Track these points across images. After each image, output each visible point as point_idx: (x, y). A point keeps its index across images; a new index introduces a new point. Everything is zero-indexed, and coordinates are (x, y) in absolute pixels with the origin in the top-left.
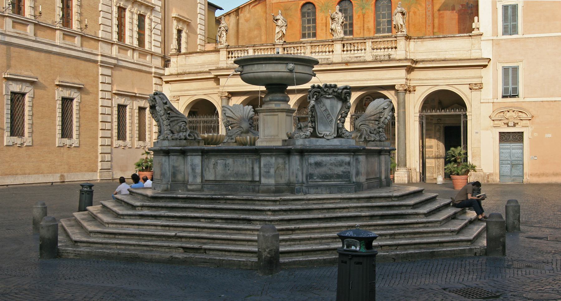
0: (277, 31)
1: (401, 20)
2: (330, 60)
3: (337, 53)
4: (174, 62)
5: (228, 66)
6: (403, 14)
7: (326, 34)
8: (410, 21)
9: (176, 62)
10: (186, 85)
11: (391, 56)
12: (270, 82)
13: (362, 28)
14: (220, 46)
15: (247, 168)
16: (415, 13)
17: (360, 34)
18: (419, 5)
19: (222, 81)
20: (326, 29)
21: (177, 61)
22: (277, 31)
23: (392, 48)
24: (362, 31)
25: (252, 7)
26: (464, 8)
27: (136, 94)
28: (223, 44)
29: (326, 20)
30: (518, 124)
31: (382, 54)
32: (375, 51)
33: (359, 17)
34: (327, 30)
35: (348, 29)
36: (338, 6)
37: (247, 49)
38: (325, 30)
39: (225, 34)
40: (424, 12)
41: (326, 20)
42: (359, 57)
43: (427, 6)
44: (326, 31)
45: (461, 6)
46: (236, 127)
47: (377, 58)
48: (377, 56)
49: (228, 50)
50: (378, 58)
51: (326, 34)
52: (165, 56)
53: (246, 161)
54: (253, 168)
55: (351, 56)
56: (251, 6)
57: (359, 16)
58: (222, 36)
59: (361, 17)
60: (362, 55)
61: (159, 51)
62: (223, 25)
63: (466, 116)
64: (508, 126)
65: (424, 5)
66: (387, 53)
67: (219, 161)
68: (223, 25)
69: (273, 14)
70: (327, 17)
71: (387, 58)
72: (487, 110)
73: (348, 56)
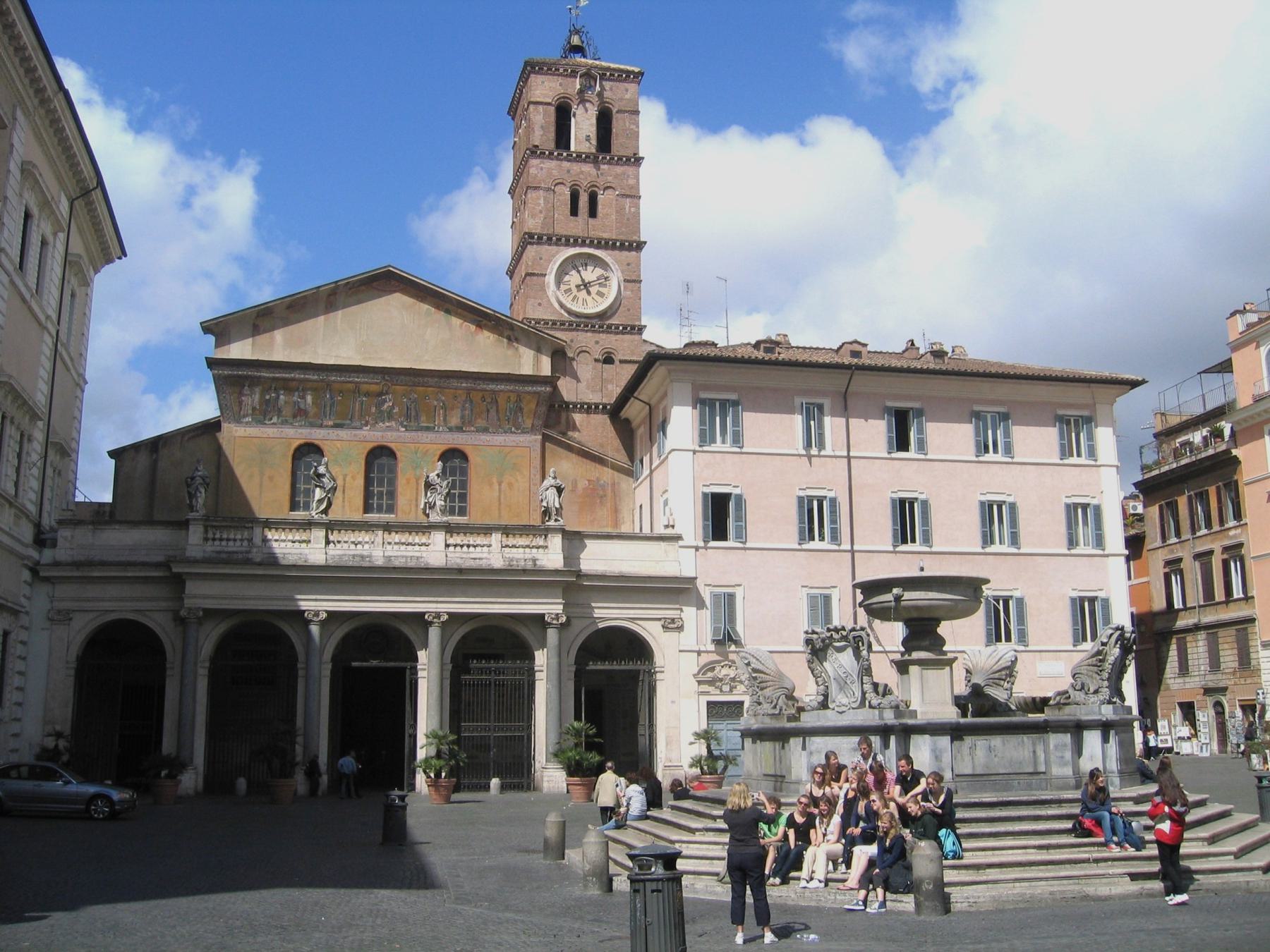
0: (317, 498)
1: (557, 499)
2: (423, 560)
3: (436, 548)
4: (65, 538)
5: (206, 555)
6: (560, 490)
7: (343, 507)
8: (502, 500)
9: (70, 538)
10: (92, 591)
11: (538, 563)
12: (915, 615)
13: (414, 502)
14: (192, 515)
15: (1026, 753)
16: (510, 485)
17: (409, 513)
18: (517, 473)
19: (191, 587)
20: (344, 498)
21: (72, 537)
22: (317, 498)
23: (462, 546)
24: (413, 509)
25: (189, 439)
26: (591, 486)
27: (7, 601)
28: (197, 511)
29: (344, 480)
30: (736, 688)
31: (521, 556)
32: (507, 550)
33: (408, 483)
34: (346, 499)
35: (457, 505)
36: (440, 463)
37: (250, 525)
38: (341, 499)
39: (203, 491)
40: (527, 485)
41: (344, 480)
42: (479, 559)
43: (532, 476)
44: (343, 502)
45: (587, 482)
46: (771, 688)
47: (512, 563)
48: (512, 560)
49: (208, 523)
50: (515, 563)
51: (343, 507)
52: (40, 522)
53: (1023, 742)
54: (1034, 752)
55: (464, 556)
56: (186, 438)
57: (408, 481)
58: (199, 495)
59: (413, 481)
60: (485, 555)
61: (32, 509)
62: (199, 473)
63: (651, 674)
64: (721, 691)
65: (526, 473)
66: (530, 556)
67: (979, 743)
68: (199, 473)
69: (315, 464)
70: (346, 475)
71: (529, 565)
72: (691, 664)
73: (457, 555)
